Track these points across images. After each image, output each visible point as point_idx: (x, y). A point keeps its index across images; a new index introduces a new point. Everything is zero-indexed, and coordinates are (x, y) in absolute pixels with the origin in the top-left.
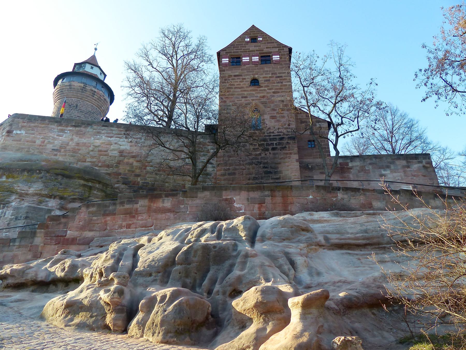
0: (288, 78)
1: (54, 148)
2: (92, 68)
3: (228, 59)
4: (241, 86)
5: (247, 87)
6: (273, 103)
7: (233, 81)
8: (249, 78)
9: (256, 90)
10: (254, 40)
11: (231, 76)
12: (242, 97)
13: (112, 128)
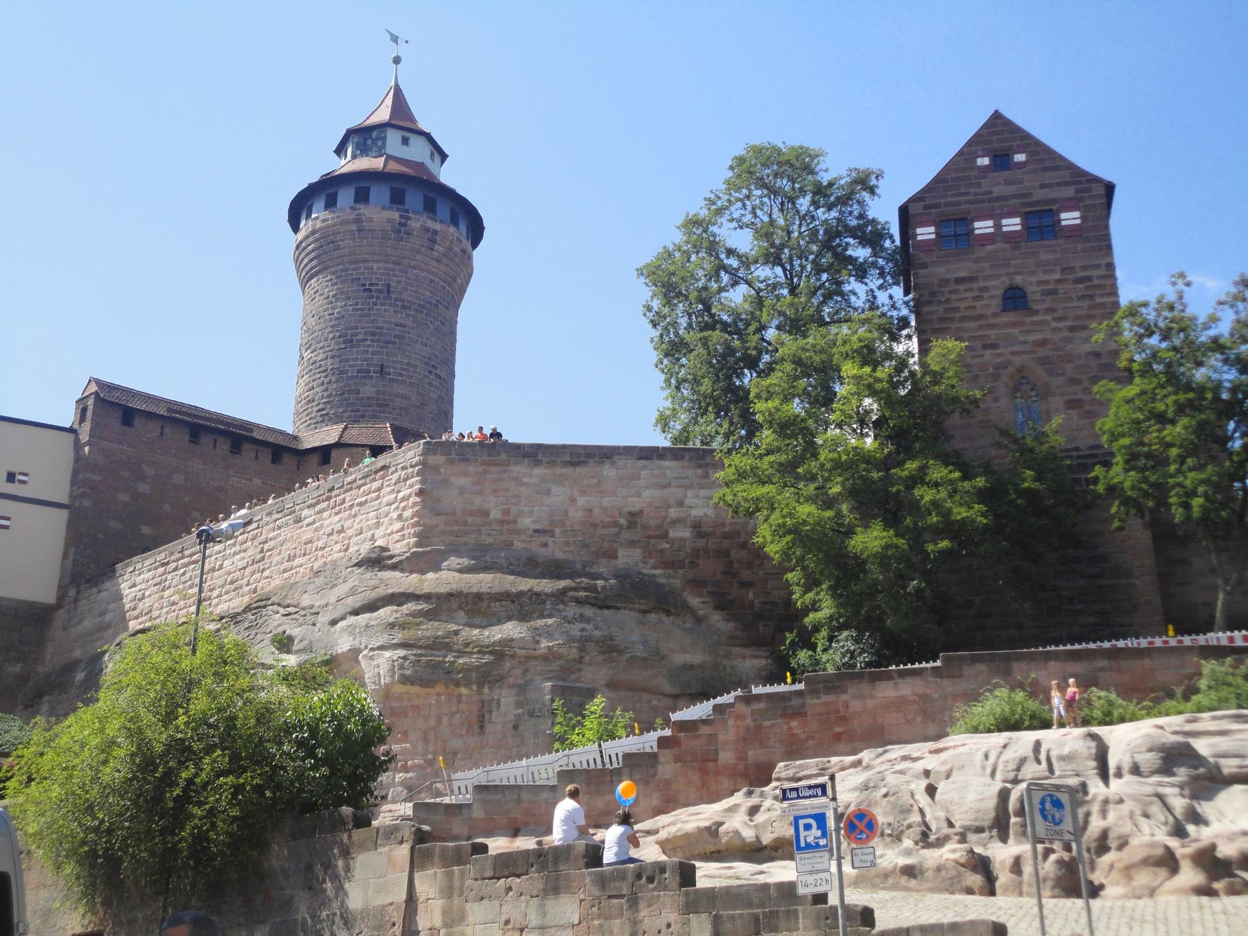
0: (1109, 282)
2: (405, 141)
3: (932, 229)
5: (995, 315)
6: (1070, 361)
7: (954, 297)
8: (995, 287)
10: (1002, 160)
11: (947, 281)
12: (985, 347)
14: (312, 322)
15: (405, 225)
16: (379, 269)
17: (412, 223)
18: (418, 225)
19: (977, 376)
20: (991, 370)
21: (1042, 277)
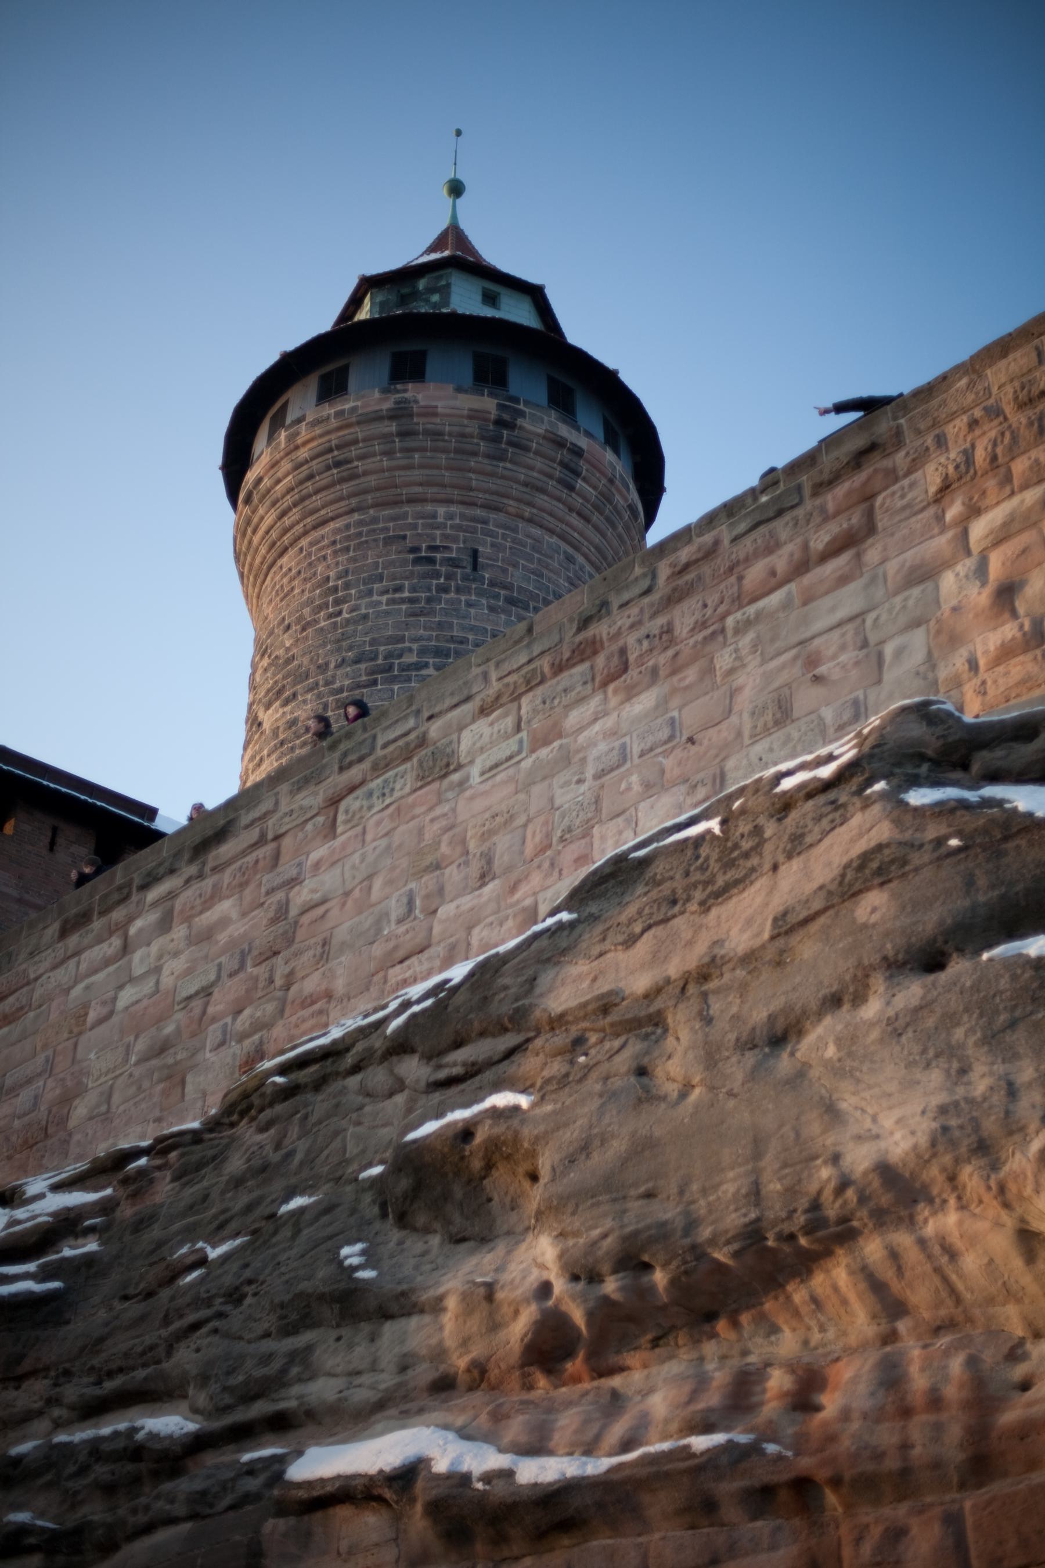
15: (511, 426)
18: (540, 430)
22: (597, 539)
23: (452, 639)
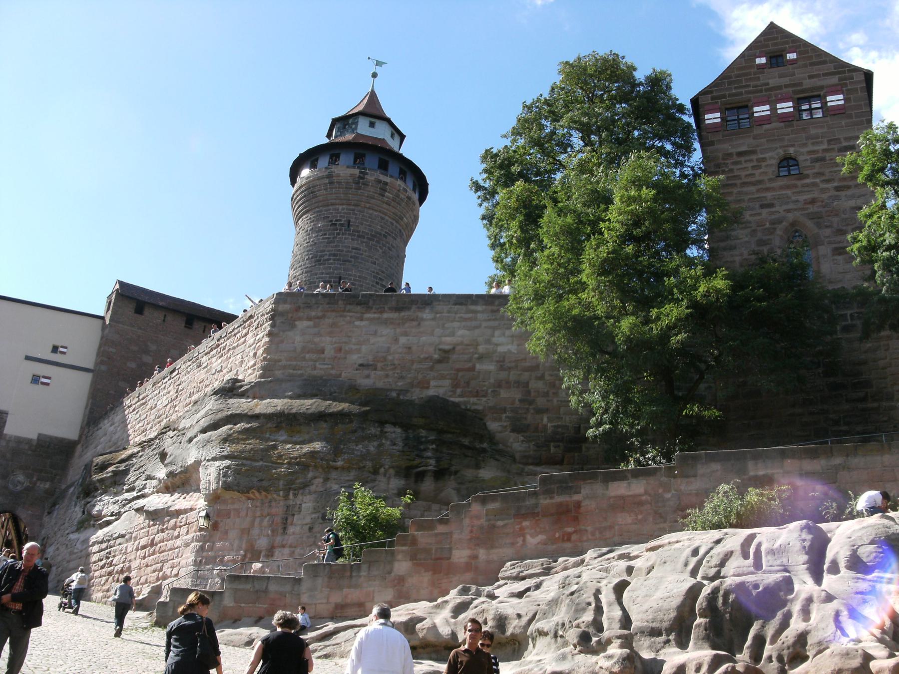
1: (360, 362)
2: (372, 125)
3: (718, 115)
4: (757, 178)
5: (770, 180)
6: (837, 215)
7: (735, 167)
8: (771, 158)
9: (795, 186)
10: (776, 59)
11: (730, 155)
12: (762, 206)
13: (473, 307)
14: (296, 248)
15: (363, 178)
16: (343, 209)
17: (368, 177)
19: (754, 231)
20: (768, 225)
21: (811, 148)
22: (393, 210)
23: (339, 250)
